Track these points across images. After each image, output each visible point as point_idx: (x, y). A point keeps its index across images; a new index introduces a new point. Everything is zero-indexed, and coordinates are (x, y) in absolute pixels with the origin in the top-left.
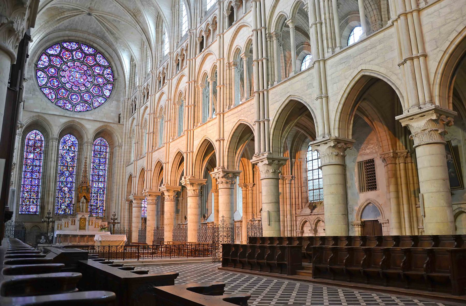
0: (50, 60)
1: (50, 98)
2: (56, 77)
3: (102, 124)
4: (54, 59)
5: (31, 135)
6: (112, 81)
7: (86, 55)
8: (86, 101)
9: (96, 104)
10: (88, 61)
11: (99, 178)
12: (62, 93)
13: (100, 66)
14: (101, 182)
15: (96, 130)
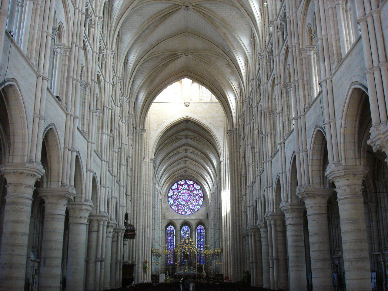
0: (173, 192)
1: (175, 210)
2: (177, 199)
3: (198, 220)
4: (175, 191)
5: (169, 228)
6: (202, 196)
7: (189, 185)
8: (191, 209)
9: (196, 209)
10: (191, 189)
11: (201, 246)
12: (180, 207)
13: (196, 189)
14: (202, 247)
15: (196, 224)
